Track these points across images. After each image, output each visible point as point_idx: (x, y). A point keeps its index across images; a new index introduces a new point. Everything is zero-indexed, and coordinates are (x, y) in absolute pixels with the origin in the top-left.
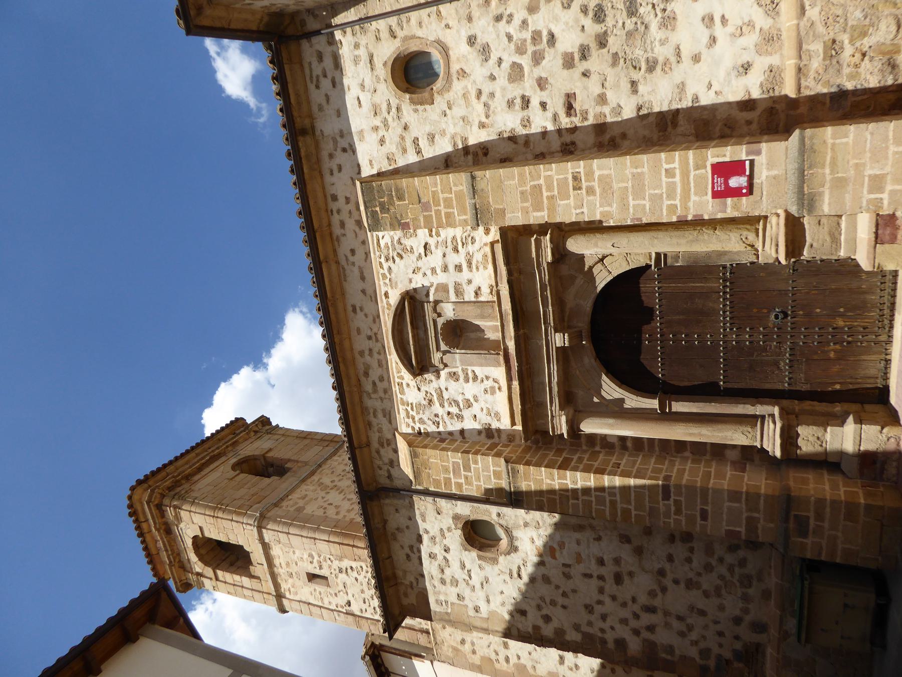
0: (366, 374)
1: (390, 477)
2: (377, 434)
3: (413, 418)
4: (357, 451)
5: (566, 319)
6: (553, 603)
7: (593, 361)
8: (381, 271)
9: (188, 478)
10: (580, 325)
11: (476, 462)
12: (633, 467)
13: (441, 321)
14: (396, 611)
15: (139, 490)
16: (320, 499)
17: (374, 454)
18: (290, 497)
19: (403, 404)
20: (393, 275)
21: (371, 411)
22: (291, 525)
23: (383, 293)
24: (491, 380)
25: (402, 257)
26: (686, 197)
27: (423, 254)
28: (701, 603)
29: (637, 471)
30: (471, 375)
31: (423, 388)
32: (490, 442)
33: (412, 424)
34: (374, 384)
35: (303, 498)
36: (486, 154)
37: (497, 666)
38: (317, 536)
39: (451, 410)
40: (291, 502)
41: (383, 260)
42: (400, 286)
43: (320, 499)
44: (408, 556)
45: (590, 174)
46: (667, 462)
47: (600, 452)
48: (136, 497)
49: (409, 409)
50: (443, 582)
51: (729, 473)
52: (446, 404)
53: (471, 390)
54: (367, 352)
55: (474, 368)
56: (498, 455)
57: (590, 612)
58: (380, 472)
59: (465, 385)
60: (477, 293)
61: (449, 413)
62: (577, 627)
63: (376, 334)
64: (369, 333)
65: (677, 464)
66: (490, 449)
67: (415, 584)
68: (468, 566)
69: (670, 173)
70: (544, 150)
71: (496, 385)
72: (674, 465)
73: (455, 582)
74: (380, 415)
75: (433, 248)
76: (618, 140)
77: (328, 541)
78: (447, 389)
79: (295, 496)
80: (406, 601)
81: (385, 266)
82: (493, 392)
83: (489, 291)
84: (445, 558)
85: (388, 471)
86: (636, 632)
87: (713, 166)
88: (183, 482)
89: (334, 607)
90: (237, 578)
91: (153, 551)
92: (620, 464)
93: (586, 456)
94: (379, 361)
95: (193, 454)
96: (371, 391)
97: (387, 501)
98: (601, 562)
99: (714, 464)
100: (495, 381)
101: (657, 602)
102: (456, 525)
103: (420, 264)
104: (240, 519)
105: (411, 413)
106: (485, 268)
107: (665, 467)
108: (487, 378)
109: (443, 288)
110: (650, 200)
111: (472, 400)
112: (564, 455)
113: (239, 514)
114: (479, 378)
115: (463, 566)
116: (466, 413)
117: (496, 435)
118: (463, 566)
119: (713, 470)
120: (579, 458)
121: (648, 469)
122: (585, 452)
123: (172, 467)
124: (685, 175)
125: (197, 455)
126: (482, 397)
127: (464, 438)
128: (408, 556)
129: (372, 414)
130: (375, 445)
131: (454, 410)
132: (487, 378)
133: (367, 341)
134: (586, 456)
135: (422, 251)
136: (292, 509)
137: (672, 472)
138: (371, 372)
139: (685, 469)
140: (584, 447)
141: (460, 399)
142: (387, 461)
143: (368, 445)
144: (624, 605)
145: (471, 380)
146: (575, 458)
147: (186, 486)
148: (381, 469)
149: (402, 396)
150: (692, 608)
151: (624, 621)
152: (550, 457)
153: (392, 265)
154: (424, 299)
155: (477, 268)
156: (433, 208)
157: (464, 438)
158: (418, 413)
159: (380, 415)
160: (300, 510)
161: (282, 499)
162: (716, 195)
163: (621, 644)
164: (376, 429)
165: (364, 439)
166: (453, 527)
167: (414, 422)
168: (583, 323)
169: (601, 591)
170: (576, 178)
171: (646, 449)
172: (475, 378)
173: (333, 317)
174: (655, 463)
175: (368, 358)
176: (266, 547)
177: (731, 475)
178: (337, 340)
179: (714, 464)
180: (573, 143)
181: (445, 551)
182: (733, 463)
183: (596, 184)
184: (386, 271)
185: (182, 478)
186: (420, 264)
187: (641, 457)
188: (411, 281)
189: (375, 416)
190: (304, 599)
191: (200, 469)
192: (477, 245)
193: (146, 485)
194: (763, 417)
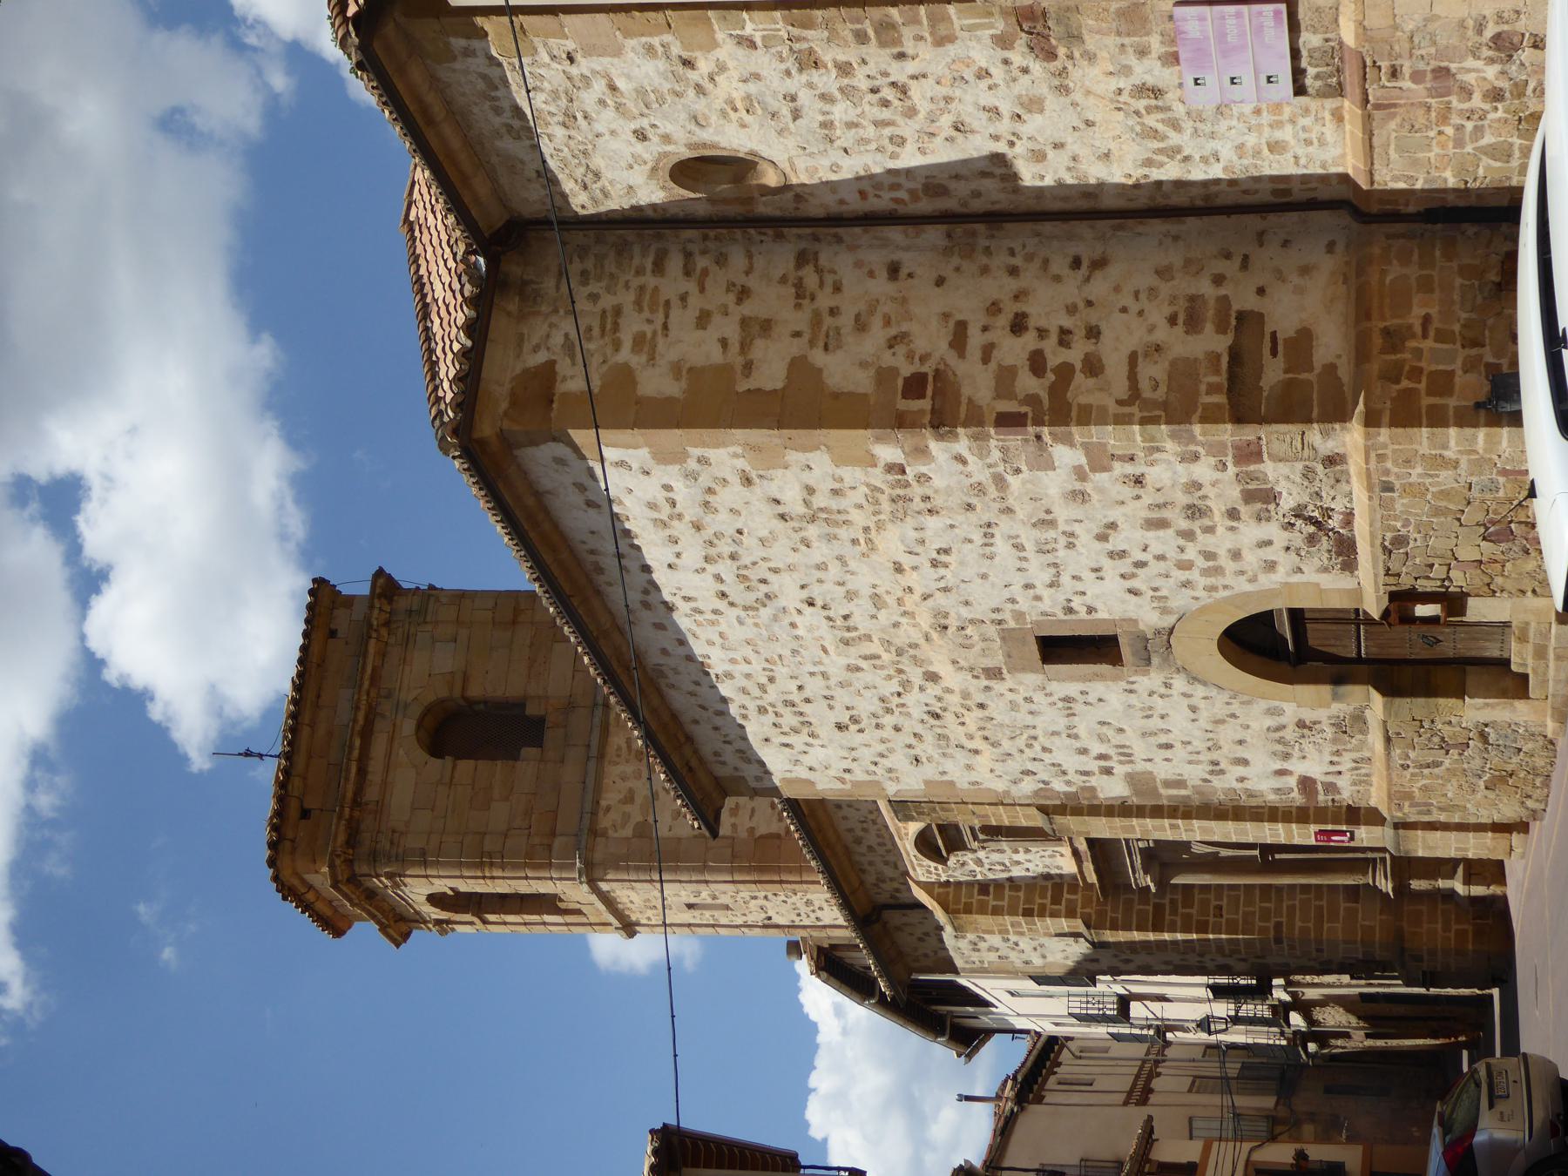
15: (285, 861)
18: (603, 803)
35: (629, 798)
38: (708, 878)
40: (614, 816)
48: (286, 874)
56: (1071, 914)
79: (610, 798)
88: (356, 814)
91: (328, 912)
92: (1221, 908)
95: (305, 731)
119: (1324, 903)
120: (1173, 902)
123: (296, 782)
125: (312, 725)
136: (628, 832)
160: (644, 831)
173: (812, 824)
193: (287, 844)
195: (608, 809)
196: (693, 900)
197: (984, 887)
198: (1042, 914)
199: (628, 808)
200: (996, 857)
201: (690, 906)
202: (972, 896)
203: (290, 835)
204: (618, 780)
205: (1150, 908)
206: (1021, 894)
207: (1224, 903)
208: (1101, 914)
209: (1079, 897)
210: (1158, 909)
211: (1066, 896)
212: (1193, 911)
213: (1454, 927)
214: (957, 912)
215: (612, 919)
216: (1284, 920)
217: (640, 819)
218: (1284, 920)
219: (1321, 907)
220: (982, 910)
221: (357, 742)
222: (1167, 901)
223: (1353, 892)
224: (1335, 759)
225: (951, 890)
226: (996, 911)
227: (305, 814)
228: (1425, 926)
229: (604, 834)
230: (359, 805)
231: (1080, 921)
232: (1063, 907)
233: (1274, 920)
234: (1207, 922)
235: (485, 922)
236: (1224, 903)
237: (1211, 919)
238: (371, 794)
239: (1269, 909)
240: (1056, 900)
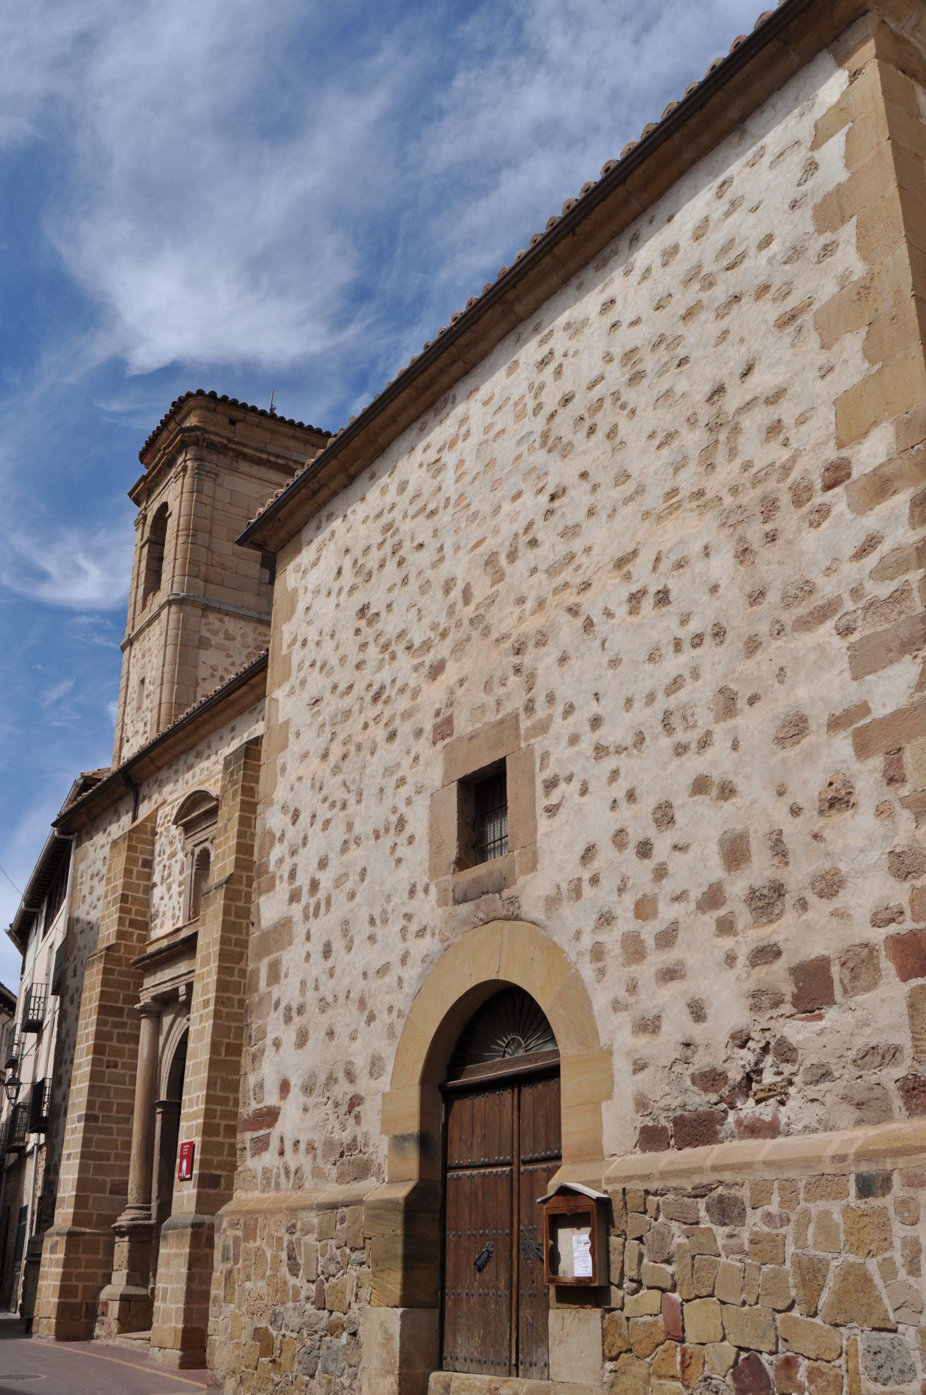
4: (146, 759)
9: (239, 455)
13: (207, 844)
16: (230, 660)
18: (226, 619)
22: (176, 645)
29: (101, 1088)
35: (229, 637)
38: (165, 686)
40: (217, 625)
43: (230, 660)
48: (192, 402)
56: (120, 935)
77: (160, 704)
79: (231, 625)
88: (231, 453)
90: (142, 578)
92: (115, 1067)
95: (290, 432)
104: (177, 572)
113: (184, 565)
125: (293, 437)
136: (204, 633)
147: (224, 461)
160: (204, 644)
161: (219, 611)
165: (159, 763)
173: (219, 707)
176: (157, 616)
177: (105, 1182)
178: (205, 716)
185: (234, 450)
191: (259, 462)
193: (213, 405)
194: (149, 1209)
195: (222, 621)
196: (147, 681)
197: (148, 864)
198: (122, 910)
199: (221, 635)
200: (176, 868)
201: (142, 682)
203: (219, 408)
204: (242, 631)
205: (120, 1005)
206: (141, 895)
207: (120, 1071)
208: (118, 961)
209: (134, 943)
210: (119, 1012)
211: (137, 932)
212: (114, 1043)
213: (80, 1285)
214: (130, 839)
215: (136, 630)
216: (100, 1124)
217: (213, 642)
218: (100, 1124)
219: (108, 1159)
220: (129, 860)
221: (280, 461)
222: (125, 1019)
223: (120, 1189)
224: (302, 1147)
225: (149, 837)
226: (128, 872)
227: (233, 422)
228: (84, 1256)
229: (203, 616)
230: (237, 457)
231: (114, 942)
232: (126, 929)
234: (103, 1053)
235: (142, 547)
236: (120, 1071)
237: (106, 1058)
238: (244, 466)
239: (111, 1111)
240: (133, 923)
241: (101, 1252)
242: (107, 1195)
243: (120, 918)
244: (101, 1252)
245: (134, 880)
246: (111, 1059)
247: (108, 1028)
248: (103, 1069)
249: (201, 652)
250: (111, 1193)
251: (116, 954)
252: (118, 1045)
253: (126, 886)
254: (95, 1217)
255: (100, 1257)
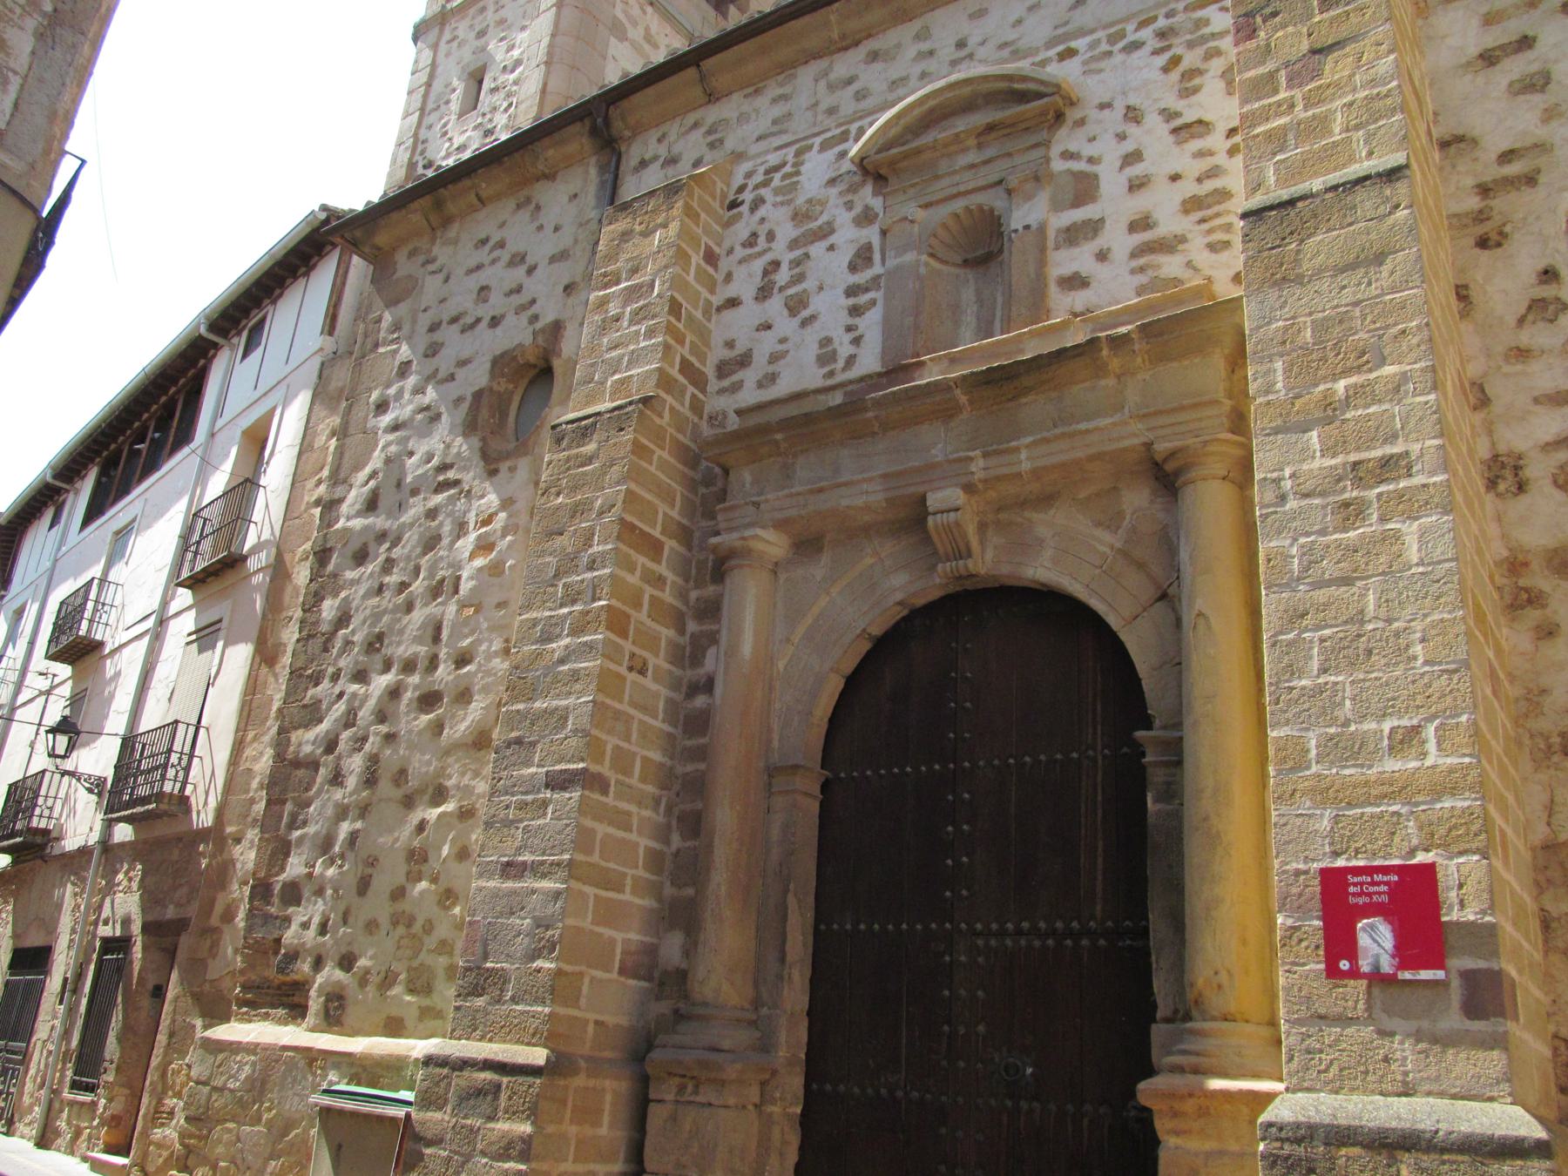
0: (874, 56)
1: (643, 164)
2: (735, 115)
3: (765, 184)
5: (1003, 516)
6: (388, 566)
7: (899, 596)
8: (1130, 27)
10: (989, 555)
11: (650, 333)
12: (634, 704)
14: (382, 239)
17: (691, 118)
18: (649, 9)
19: (798, 154)
20: (1119, 58)
21: (787, 90)
23: (1073, 44)
24: (851, 350)
25: (1166, 70)
26: (1323, 793)
27: (1178, 122)
28: (383, 883)
29: (618, 715)
30: (864, 299)
31: (833, 191)
32: (709, 370)
33: (751, 183)
34: (850, 81)
36: (1483, 243)
37: (311, 483)
39: (784, 267)
41: (1162, 23)
42: (1091, 81)
44: (484, 242)
45: (1407, 505)
46: (650, 789)
47: (681, 631)
49: (788, 169)
50: (433, 328)
51: (619, 936)
52: (798, 253)
53: (830, 307)
54: (925, 46)
55: (880, 304)
56: (665, 381)
57: (370, 644)
58: (654, 140)
59: (840, 291)
60: (1076, 282)
61: (776, 264)
62: (343, 619)
63: (971, 56)
64: (972, 42)
65: (647, 813)
66: (686, 367)
67: (431, 267)
68: (461, 374)
69: (1407, 740)
70: (1497, 407)
71: (840, 364)
72: (640, 804)
73: (433, 351)
74: (778, 111)
75: (1195, 145)
76: (1533, 615)
78: (831, 248)
80: (401, 257)
81: (1146, 34)
82: (826, 357)
83: (1079, 308)
84: (478, 320)
85: (656, 158)
86: (331, 745)
87: (1430, 869)
89: (422, 137)
92: (642, 672)
93: (667, 596)
94: (904, 80)
96: (832, 76)
97: (593, 171)
98: (462, 660)
99: (648, 902)
100: (851, 361)
101: (385, 787)
102: (543, 330)
103: (1153, 120)
105: (778, 176)
106: (1140, 291)
107: (634, 781)
108: (857, 341)
109: (1084, 189)
110: (1321, 689)
111: (805, 313)
112: (670, 545)
114: (857, 321)
115: (462, 363)
116: (775, 307)
117: (726, 383)
118: (462, 363)
119: (627, 896)
121: (628, 739)
122: (683, 595)
124: (1398, 789)
126: (812, 335)
127: (719, 309)
128: (484, 242)
129: (780, 91)
130: (712, 114)
131: (783, 276)
132: (857, 341)
133: (952, 41)
134: (667, 596)
135: (1189, 117)
137: (618, 796)
138: (878, 66)
139: (629, 829)
140: (694, 595)
141: (809, 284)
142: (676, 149)
143: (712, 97)
144: (381, 717)
145: (851, 301)
146: (663, 569)
148: (659, 141)
149: (816, 148)
150: (372, 862)
151: (349, 720)
152: (662, 508)
153: (1148, 49)
154: (1055, 151)
155: (1142, 270)
156: (1298, 94)
157: (719, 309)
158: (777, 191)
159: (778, 111)
162: (1333, 881)
163: (313, 714)
164: (746, 107)
166: (539, 325)
167: (756, 187)
168: (989, 561)
169: (409, 667)
170: (1389, 467)
171: (689, 743)
172: (855, 311)
174: (645, 759)
175: (911, 52)
177: (612, 941)
179: (648, 902)
180: (1521, 487)
181: (493, 318)
182: (651, 951)
183: (1371, 526)
184: (1131, 38)
186: (1153, 120)
187: (667, 728)
188: (1103, 106)
189: (775, 101)
190: (439, 70)
192: (1203, 258)
200: (830, 267)
202: (707, 232)
206: (698, 314)
212: (643, 616)
216: (610, 800)
217: (630, 35)
218: (610, 800)
226: (682, 257)
232: (675, 372)
233: (613, 777)
234: (623, 634)
237: (628, 646)
241: (606, 1119)
242: (614, 975)
243: (667, 347)
244: (606, 1119)
245: (691, 278)
246: (638, 651)
247: (634, 579)
248: (623, 670)
249: (613, 40)
250: (622, 971)
251: (658, 421)
252: (649, 622)
253: (677, 283)
254: (591, 1028)
255: (604, 1131)
